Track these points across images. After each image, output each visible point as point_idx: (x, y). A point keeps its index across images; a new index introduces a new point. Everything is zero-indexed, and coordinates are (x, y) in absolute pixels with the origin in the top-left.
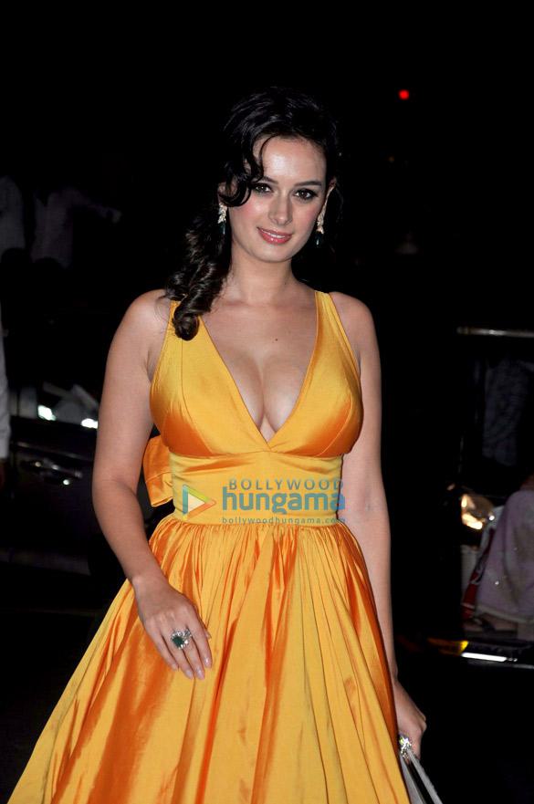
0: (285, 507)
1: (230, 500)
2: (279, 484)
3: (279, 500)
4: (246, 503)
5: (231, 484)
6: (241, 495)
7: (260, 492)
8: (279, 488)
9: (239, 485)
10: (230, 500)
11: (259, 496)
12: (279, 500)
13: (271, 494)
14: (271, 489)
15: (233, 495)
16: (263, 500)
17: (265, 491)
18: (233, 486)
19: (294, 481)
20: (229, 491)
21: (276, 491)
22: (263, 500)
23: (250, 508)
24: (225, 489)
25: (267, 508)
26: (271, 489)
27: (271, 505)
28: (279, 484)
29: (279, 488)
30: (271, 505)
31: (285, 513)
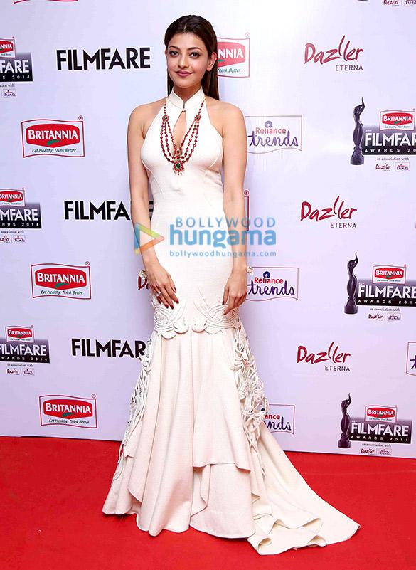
0: (225, 242)
1: (176, 236)
2: (219, 222)
3: (219, 236)
4: (191, 239)
5: (177, 222)
6: (187, 232)
7: (202, 229)
8: (219, 226)
9: (184, 222)
10: (176, 236)
11: (201, 233)
12: (219, 236)
13: (212, 231)
14: (212, 226)
15: (180, 233)
16: (205, 236)
17: (207, 228)
18: (179, 224)
19: (232, 220)
20: (175, 228)
21: (216, 228)
22: (205, 236)
23: (194, 242)
24: (172, 226)
25: (209, 243)
26: (212, 226)
27: (212, 240)
28: (219, 222)
29: (219, 226)
30: (212, 240)
31: (224, 247)
